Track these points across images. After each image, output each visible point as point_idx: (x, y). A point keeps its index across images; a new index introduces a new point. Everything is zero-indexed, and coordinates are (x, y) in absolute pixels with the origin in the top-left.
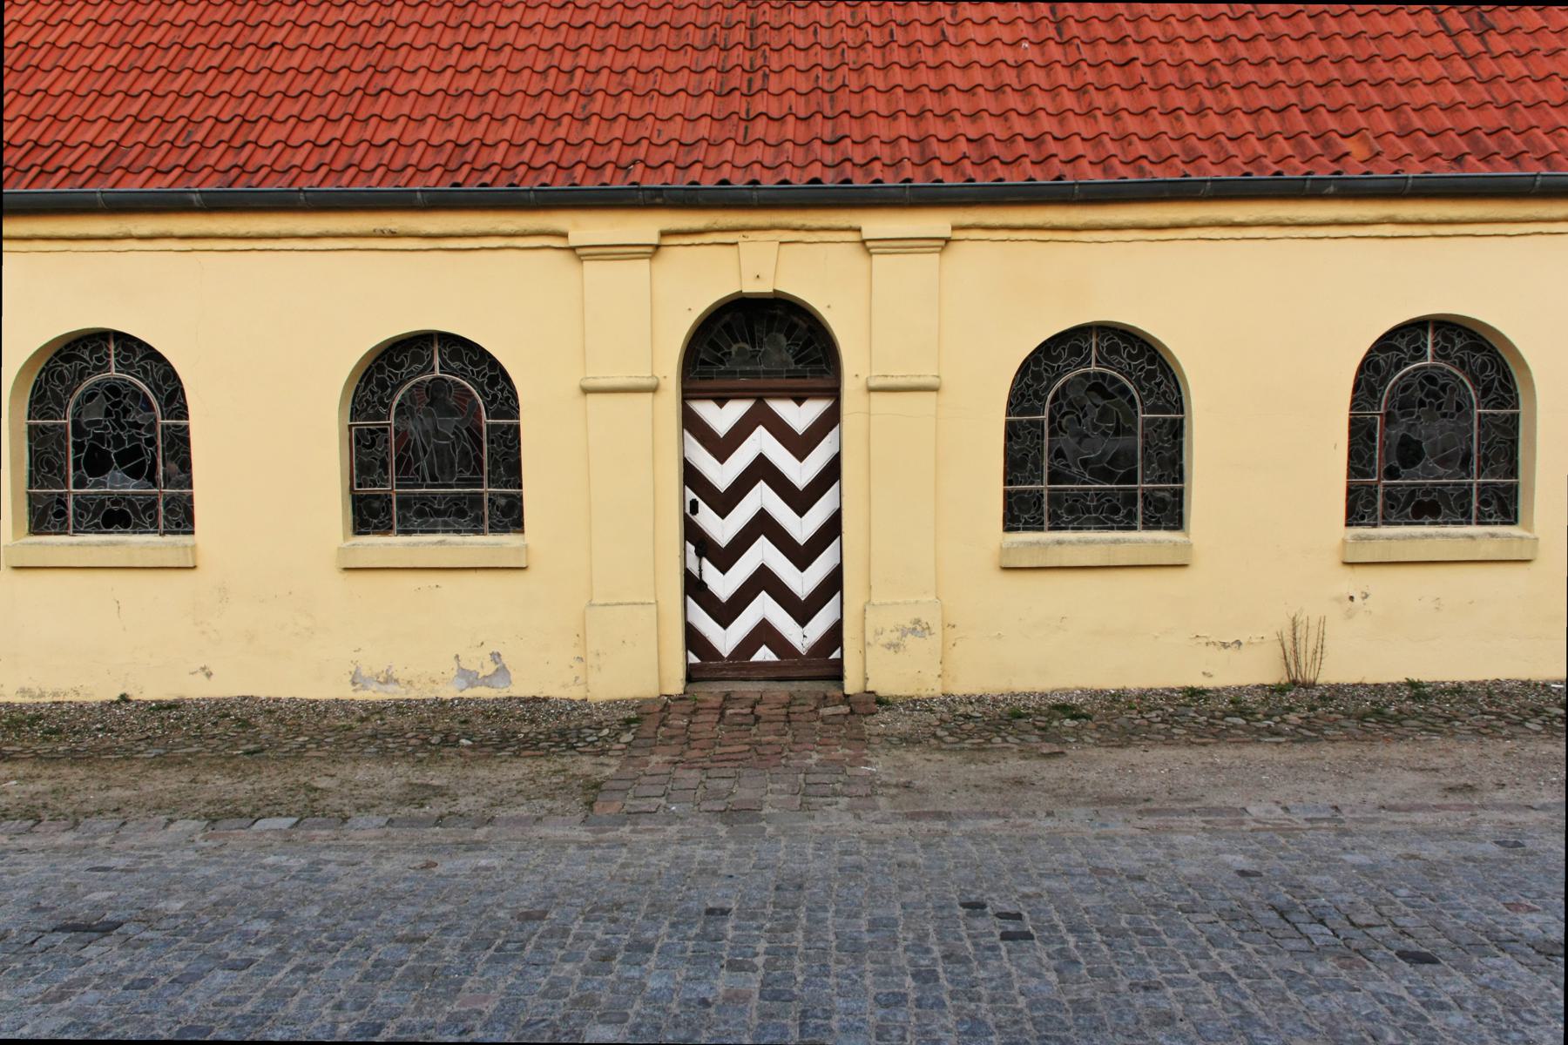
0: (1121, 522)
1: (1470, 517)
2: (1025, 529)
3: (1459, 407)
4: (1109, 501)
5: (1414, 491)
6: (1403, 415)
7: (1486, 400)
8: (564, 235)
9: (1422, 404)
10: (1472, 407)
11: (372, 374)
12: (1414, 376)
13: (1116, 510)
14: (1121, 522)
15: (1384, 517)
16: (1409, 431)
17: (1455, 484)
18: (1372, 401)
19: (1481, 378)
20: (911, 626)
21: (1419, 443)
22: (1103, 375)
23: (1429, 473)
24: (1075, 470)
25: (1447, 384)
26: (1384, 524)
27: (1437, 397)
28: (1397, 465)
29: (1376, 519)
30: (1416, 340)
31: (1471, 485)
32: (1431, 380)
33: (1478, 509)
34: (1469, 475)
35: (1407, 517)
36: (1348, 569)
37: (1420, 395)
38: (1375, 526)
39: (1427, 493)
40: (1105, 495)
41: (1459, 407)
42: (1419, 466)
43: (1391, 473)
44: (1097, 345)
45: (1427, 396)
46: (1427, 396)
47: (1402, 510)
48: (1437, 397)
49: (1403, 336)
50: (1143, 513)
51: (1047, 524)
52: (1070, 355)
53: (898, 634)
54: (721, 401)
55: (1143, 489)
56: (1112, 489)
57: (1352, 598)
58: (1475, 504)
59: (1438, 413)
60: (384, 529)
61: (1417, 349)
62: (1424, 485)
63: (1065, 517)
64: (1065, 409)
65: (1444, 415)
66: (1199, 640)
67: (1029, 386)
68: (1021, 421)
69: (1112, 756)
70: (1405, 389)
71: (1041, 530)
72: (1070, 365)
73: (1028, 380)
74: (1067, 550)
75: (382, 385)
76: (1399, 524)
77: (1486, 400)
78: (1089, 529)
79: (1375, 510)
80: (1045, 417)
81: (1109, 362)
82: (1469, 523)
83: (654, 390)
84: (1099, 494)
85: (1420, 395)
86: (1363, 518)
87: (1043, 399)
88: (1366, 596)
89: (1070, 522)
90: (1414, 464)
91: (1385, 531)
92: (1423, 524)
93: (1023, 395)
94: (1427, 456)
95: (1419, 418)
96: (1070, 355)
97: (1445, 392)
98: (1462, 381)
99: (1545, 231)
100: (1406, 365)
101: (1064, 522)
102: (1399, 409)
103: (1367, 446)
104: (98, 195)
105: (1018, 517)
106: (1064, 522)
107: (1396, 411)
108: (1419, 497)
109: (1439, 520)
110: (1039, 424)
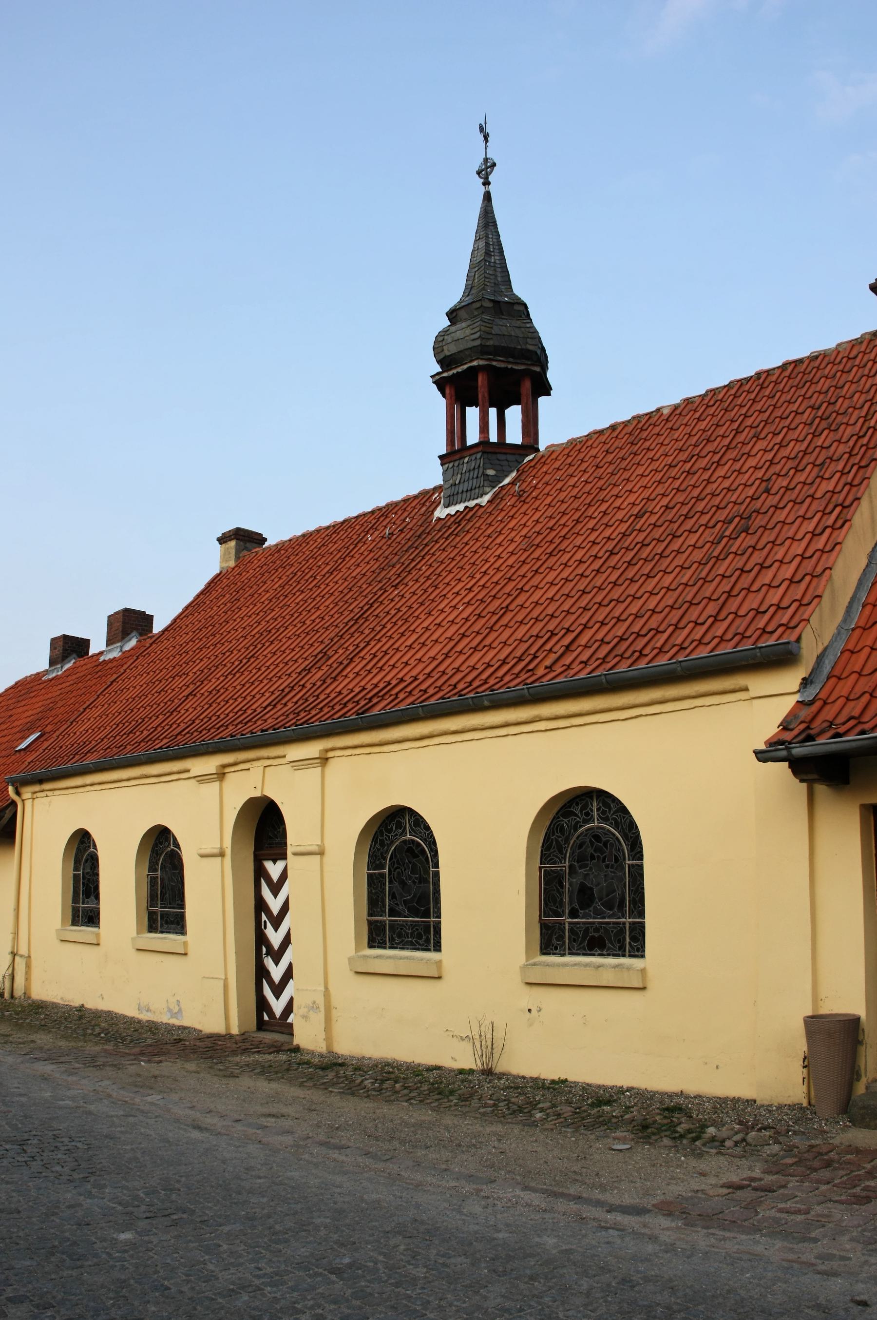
0: (423, 945)
1: (625, 951)
2: (379, 947)
3: (617, 860)
4: (417, 930)
5: (588, 927)
6: (580, 868)
7: (633, 853)
8: (188, 771)
9: (592, 857)
10: (624, 859)
11: (377, 837)
12: (586, 835)
13: (420, 936)
14: (423, 945)
15: (569, 949)
16: (585, 879)
17: (614, 923)
18: (560, 856)
19: (630, 835)
20: (312, 1005)
21: (592, 889)
22: (413, 841)
23: (598, 914)
24: (401, 907)
25: (608, 841)
26: (570, 954)
27: (602, 852)
28: (577, 907)
29: (564, 950)
30: (585, 807)
31: (624, 923)
32: (597, 838)
33: (630, 943)
34: (624, 916)
35: (585, 950)
36: (528, 988)
37: (591, 850)
38: (563, 955)
39: (597, 930)
40: (416, 926)
41: (617, 860)
42: (592, 908)
43: (573, 914)
44: (409, 820)
45: (595, 851)
46: (595, 851)
47: (581, 944)
48: (602, 852)
49: (577, 804)
50: (434, 939)
51: (388, 945)
52: (397, 828)
53: (306, 1010)
54: (274, 862)
55: (433, 921)
56: (418, 921)
57: (530, 1010)
58: (628, 940)
59: (603, 865)
60: (382, 945)
61: (587, 814)
62: (593, 923)
63: (397, 940)
64: (396, 865)
65: (607, 866)
66: (448, 1033)
67: (378, 850)
68: (375, 874)
69: (702, 1165)
70: (580, 846)
71: (385, 948)
72: (396, 835)
73: (378, 846)
74: (377, 962)
75: (382, 844)
76: (578, 954)
77: (633, 853)
78: (407, 949)
79: (564, 943)
80: (386, 871)
81: (415, 832)
82: (624, 956)
83: (295, 854)
84: (414, 925)
85: (591, 850)
86: (556, 948)
87: (385, 859)
88: (540, 1011)
89: (399, 944)
90: (589, 906)
91: (568, 959)
92: (594, 955)
93: (376, 856)
94: (597, 900)
95: (591, 869)
96: (397, 828)
97: (607, 848)
98: (617, 838)
99: (535, 729)
100: (581, 826)
101: (396, 943)
102: (578, 862)
103: (558, 891)
104: (91, 765)
105: (375, 938)
106: (396, 943)
107: (576, 864)
108: (592, 933)
109: (605, 952)
110: (383, 875)
